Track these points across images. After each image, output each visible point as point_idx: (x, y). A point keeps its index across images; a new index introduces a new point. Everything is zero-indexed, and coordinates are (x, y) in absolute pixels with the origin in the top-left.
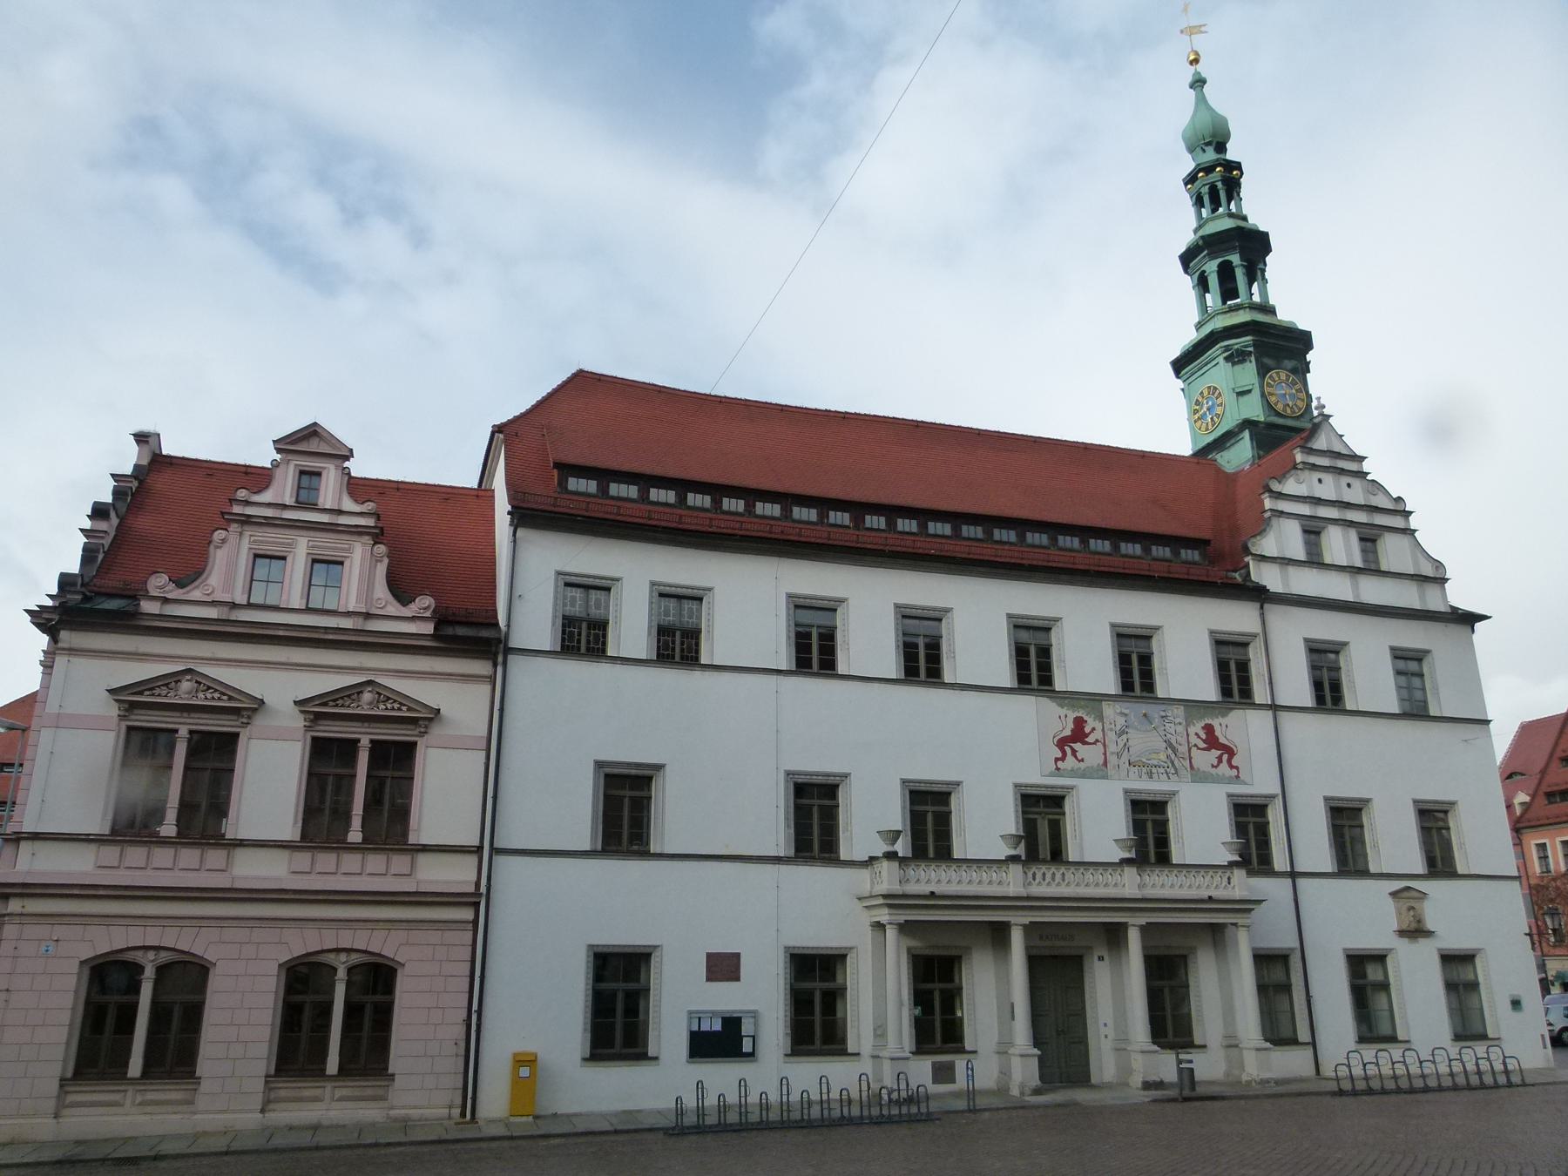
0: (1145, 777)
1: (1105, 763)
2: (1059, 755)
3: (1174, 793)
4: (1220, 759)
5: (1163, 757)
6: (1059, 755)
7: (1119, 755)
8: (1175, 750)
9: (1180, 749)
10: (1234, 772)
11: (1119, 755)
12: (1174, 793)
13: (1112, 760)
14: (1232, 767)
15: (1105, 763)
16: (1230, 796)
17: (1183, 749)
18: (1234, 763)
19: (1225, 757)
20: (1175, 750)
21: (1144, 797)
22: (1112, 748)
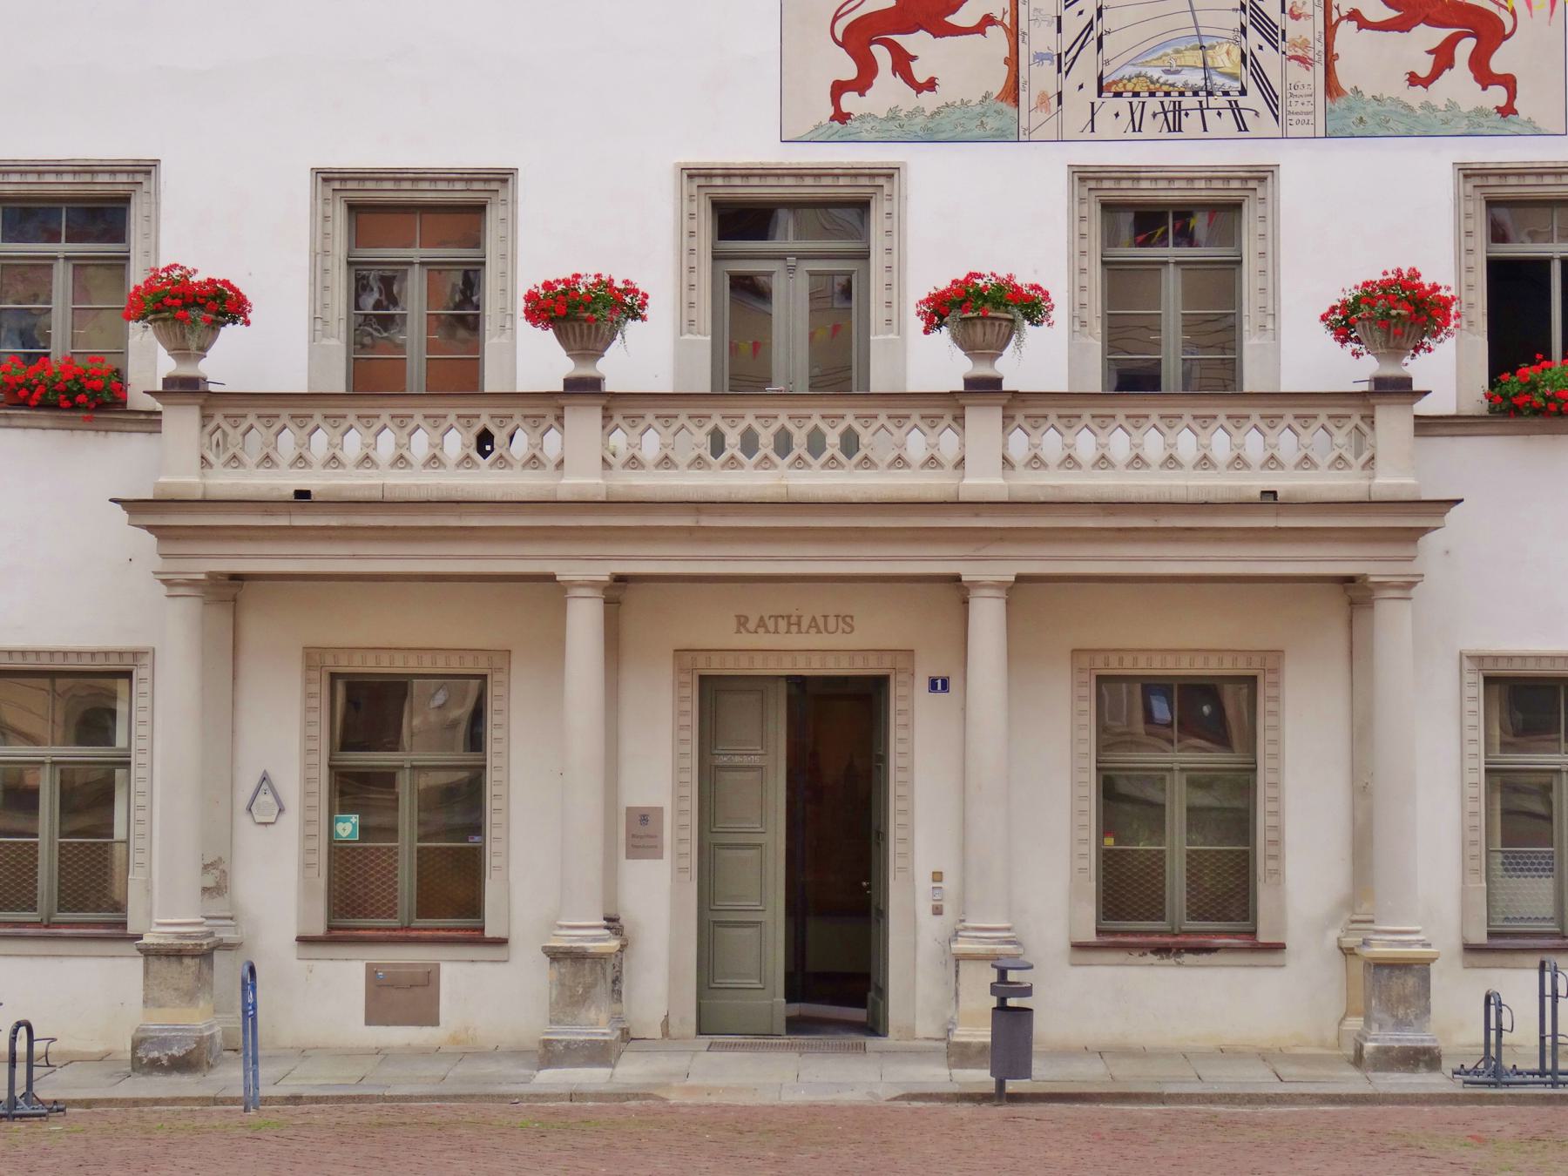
0: (1152, 127)
1: (1012, 91)
2: (849, 71)
3: (1262, 176)
4: (1443, 57)
5: (1224, 58)
6: (849, 71)
7: (1063, 64)
8: (1272, 34)
9: (1294, 29)
10: (1498, 95)
11: (1063, 64)
12: (1262, 176)
13: (1039, 79)
14: (1484, 77)
15: (1012, 91)
16: (1468, 173)
17: (1306, 31)
18: (1499, 63)
19: (1466, 47)
20: (1272, 34)
21: (1147, 192)
22: (1040, 38)
